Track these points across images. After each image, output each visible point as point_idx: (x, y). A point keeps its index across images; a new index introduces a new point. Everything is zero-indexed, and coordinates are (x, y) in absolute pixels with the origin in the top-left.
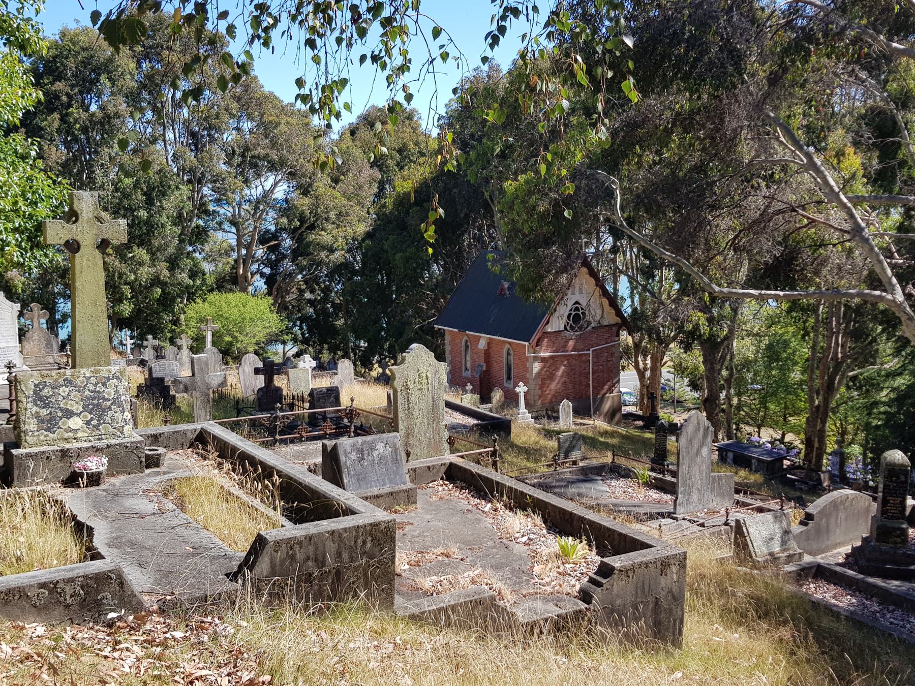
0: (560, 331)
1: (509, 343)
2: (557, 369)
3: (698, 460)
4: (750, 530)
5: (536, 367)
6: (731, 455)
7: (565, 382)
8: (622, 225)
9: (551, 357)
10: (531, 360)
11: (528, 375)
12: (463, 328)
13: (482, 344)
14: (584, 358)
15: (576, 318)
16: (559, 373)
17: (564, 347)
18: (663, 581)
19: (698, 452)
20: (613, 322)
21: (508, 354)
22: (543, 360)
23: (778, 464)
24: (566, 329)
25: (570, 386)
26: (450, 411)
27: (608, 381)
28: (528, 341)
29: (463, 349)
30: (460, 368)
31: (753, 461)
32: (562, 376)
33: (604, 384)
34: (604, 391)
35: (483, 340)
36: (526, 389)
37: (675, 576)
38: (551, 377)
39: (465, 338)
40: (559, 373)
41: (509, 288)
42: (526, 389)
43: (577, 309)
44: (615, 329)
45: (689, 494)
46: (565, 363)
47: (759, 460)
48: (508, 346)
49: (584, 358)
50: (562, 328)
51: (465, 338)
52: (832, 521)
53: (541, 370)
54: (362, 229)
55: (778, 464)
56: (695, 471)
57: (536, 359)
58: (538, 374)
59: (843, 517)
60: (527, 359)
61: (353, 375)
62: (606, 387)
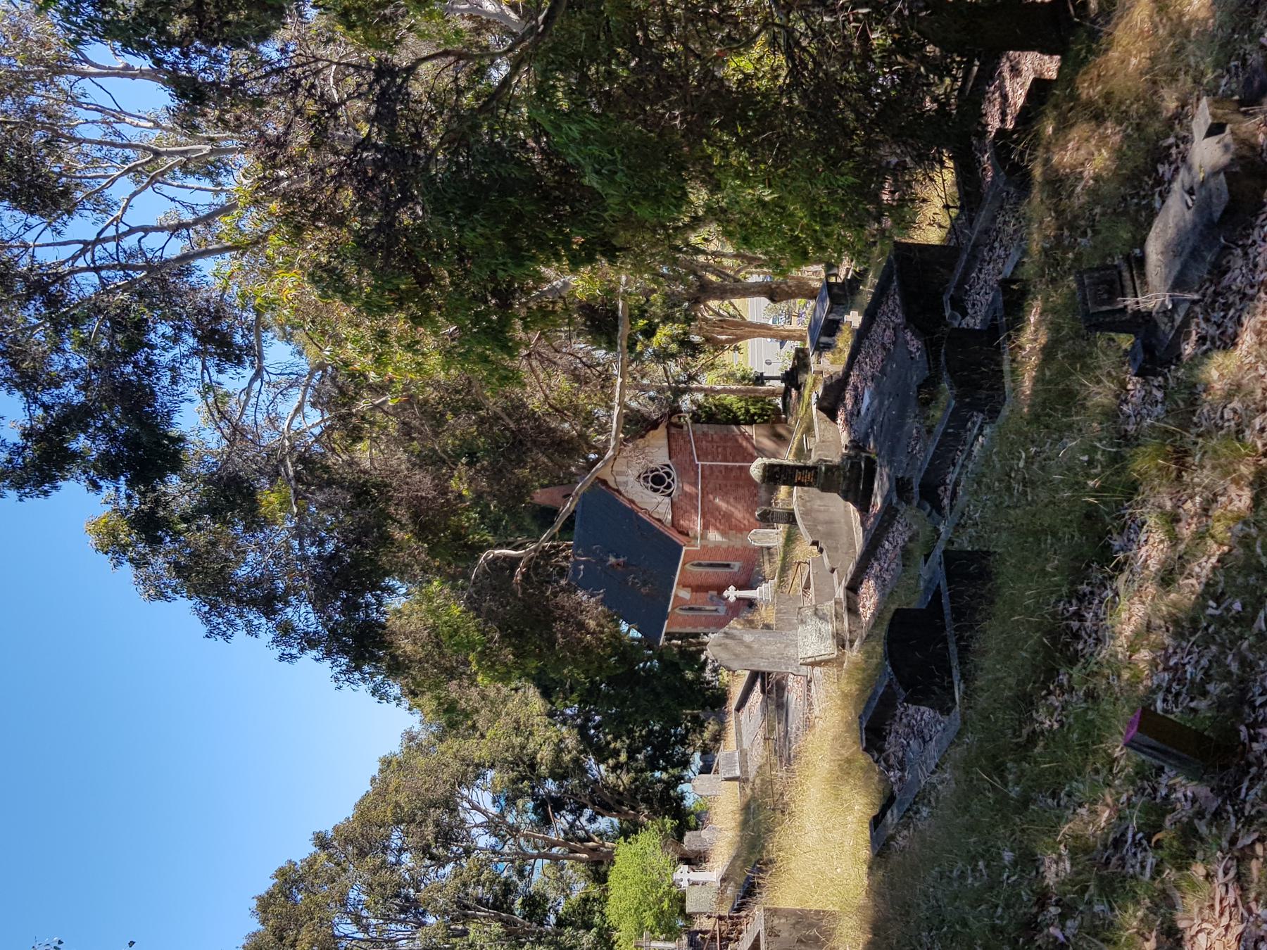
0: (673, 504)
1: (684, 564)
2: (718, 509)
3: (756, 646)
4: (810, 654)
5: (714, 536)
6: (824, 339)
7: (735, 498)
8: (535, 550)
9: (703, 516)
10: (704, 542)
11: (725, 546)
12: (664, 615)
13: (685, 594)
14: (707, 472)
15: (657, 481)
16: (723, 505)
17: (691, 498)
18: (784, 935)
19: (749, 647)
20: (665, 433)
21: (699, 565)
22: (706, 527)
23: (835, 290)
24: (669, 495)
25: (741, 491)
26: (748, 705)
27: (737, 441)
28: (680, 548)
29: (690, 613)
30: (715, 617)
31: (831, 317)
32: (728, 502)
33: (741, 446)
34: (749, 447)
35: (680, 593)
36: (732, 588)
37: (783, 921)
38: (727, 516)
39: (677, 611)
40: (723, 505)
41: (617, 557)
42: (732, 588)
43: (646, 478)
44: (673, 430)
45: (789, 658)
46: (711, 497)
47: (830, 312)
48: (687, 566)
49: (707, 472)
50: (667, 500)
51: (677, 611)
52: (821, 517)
53: (717, 529)
54: (537, 703)
55: (835, 290)
56: (767, 650)
57: (704, 537)
58: (723, 534)
59: (818, 502)
60: (703, 547)
61: (711, 775)
62: (745, 444)
